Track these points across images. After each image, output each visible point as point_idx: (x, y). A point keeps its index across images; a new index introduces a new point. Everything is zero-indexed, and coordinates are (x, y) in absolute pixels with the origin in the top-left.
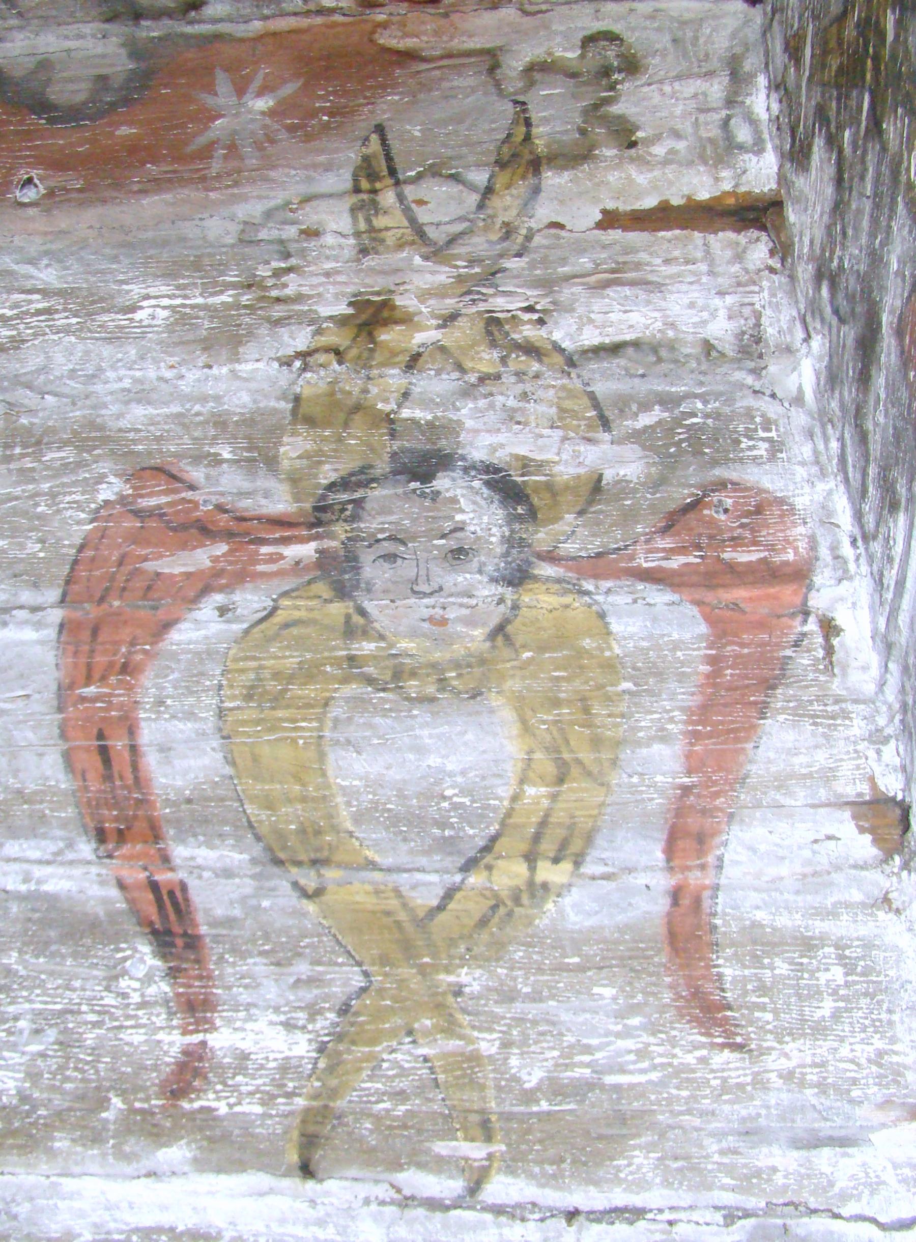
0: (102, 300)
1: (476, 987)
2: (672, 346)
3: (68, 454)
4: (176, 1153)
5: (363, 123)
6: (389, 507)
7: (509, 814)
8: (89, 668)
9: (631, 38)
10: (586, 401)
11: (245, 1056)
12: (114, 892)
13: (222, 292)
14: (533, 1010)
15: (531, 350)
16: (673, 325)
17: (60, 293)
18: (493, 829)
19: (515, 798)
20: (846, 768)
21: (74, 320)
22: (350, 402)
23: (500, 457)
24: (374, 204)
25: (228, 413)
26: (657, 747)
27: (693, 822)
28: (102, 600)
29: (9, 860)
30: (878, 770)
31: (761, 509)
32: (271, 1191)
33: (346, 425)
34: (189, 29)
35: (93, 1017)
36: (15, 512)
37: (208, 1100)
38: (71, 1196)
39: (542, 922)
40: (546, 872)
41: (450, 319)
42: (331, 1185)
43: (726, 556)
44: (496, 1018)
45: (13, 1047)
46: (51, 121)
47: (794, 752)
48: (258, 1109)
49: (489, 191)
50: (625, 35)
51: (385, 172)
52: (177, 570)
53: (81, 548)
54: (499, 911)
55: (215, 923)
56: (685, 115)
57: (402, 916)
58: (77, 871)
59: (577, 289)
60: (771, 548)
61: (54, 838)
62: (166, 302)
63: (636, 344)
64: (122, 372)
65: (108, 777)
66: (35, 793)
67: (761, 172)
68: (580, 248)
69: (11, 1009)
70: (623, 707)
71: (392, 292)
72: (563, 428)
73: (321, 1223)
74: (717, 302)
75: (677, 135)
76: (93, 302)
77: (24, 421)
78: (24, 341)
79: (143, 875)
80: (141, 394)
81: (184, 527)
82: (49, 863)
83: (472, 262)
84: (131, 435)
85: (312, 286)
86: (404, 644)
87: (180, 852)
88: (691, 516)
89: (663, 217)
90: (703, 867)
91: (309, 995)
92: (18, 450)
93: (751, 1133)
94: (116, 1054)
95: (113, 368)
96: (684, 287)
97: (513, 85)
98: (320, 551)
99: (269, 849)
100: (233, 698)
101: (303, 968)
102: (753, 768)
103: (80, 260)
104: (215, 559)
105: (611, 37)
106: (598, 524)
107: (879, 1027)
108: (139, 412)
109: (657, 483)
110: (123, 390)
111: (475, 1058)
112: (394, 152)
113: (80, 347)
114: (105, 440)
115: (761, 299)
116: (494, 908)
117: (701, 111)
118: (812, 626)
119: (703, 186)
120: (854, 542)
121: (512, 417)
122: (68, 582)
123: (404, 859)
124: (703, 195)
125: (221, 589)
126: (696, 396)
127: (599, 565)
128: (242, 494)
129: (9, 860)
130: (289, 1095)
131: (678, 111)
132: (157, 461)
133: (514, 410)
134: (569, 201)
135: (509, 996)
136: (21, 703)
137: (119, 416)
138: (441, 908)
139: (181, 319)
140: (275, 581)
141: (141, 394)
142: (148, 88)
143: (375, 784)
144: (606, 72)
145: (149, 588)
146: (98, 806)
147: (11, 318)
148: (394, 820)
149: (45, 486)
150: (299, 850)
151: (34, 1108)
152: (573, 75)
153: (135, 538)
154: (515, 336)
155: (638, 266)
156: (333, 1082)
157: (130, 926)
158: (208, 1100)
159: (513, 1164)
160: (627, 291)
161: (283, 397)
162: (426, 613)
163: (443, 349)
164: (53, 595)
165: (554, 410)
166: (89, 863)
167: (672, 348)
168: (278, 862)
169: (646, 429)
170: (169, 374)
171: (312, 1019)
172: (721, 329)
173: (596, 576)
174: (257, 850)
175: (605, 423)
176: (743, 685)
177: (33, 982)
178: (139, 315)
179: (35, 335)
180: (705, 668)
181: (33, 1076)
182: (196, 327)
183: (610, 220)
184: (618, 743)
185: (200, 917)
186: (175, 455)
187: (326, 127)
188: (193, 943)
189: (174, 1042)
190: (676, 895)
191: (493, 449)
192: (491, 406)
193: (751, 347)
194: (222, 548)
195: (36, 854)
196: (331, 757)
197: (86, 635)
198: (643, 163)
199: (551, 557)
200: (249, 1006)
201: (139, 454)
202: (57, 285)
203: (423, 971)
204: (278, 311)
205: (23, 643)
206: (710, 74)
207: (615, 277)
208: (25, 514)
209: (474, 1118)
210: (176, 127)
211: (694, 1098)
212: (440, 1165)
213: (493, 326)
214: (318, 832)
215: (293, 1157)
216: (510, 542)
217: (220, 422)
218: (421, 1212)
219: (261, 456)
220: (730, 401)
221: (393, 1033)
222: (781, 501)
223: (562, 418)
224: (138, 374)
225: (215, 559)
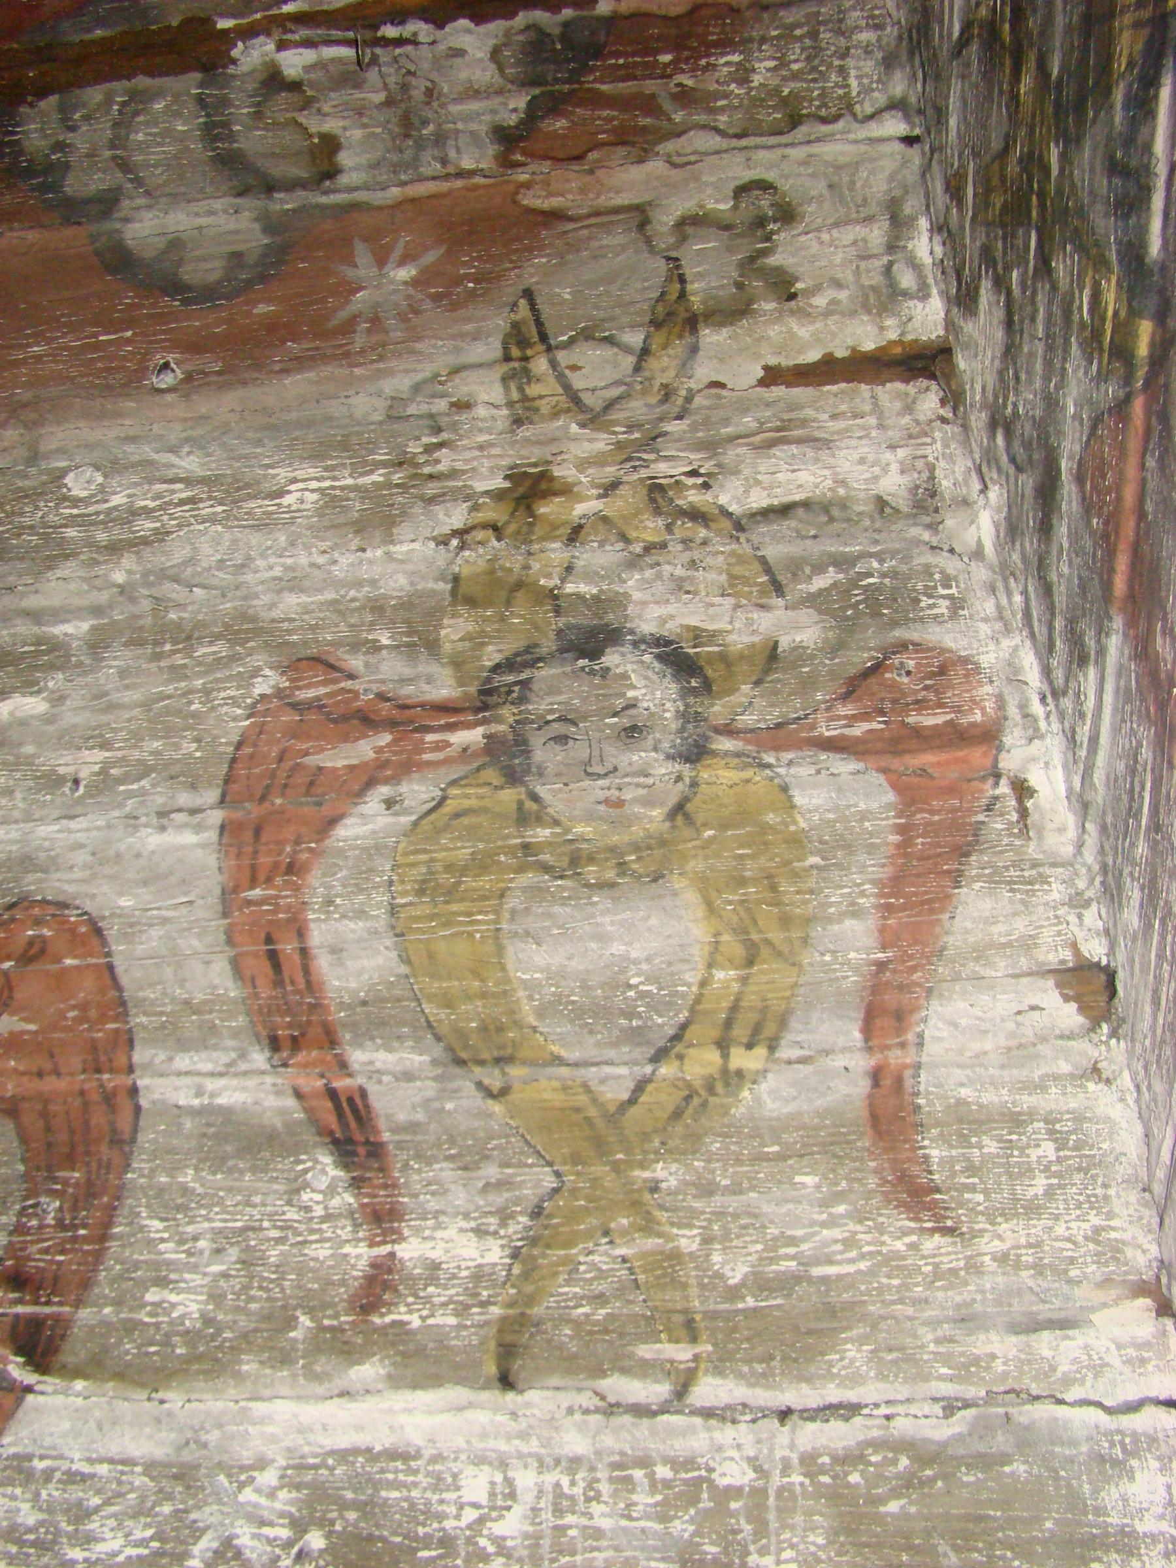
0: (248, 486)
1: (673, 1182)
2: (843, 505)
3: (220, 648)
4: (368, 1371)
5: (510, 289)
6: (556, 688)
7: (698, 1000)
8: (254, 869)
9: (784, 185)
10: (757, 566)
11: (435, 1266)
12: (291, 1102)
13: (372, 472)
14: (734, 1203)
15: (697, 515)
16: (843, 483)
17: (203, 481)
18: (682, 1017)
19: (703, 983)
20: (1047, 935)
21: (220, 509)
22: (512, 579)
23: (670, 629)
24: (526, 372)
25: (385, 597)
26: (848, 923)
27: (890, 999)
28: (263, 798)
29: (179, 1074)
30: (1080, 936)
31: (946, 669)
32: (470, 1405)
33: (508, 603)
34: (324, 200)
35: (275, 1234)
36: (168, 711)
37: (399, 1314)
38: (262, 1421)
39: (738, 1111)
40: (740, 1059)
41: (610, 488)
42: (532, 1395)
43: (910, 720)
44: (695, 1214)
45: (194, 1269)
46: (186, 302)
47: (992, 920)
48: (452, 1321)
49: (645, 352)
50: (779, 183)
51: (536, 339)
52: (339, 764)
53: (239, 745)
54: (693, 1102)
55: (397, 1129)
56: (845, 263)
57: (593, 1112)
58: (252, 1082)
60: (958, 709)
61: (225, 1049)
62: (314, 485)
63: (806, 504)
64: (272, 560)
65: (279, 983)
66: (204, 1002)
67: (928, 318)
68: (743, 407)
69: (190, 1229)
70: (811, 883)
71: (549, 463)
72: (735, 595)
73: (524, 1436)
74: (888, 456)
75: (838, 284)
76: (239, 489)
77: (173, 616)
78: (168, 533)
79: (320, 1083)
80: (293, 582)
81: (345, 718)
82: (221, 1075)
83: (631, 428)
84: (285, 625)
85: (466, 461)
86: (579, 829)
87: (357, 1057)
88: (872, 680)
89: (826, 371)
90: (903, 1045)
91: (499, 1199)
92: (168, 647)
93: (967, 1319)
94: (301, 1270)
95: (263, 556)
96: (853, 443)
97: (664, 239)
98: (488, 737)
99: (450, 1049)
100: (405, 893)
101: (491, 1171)
102: (950, 940)
103: (223, 445)
104: (379, 750)
105: (764, 186)
106: (776, 693)
107: (1097, 1203)
108: (292, 601)
109: (835, 648)
110: (275, 579)
111: (675, 1256)
112: (544, 316)
113: (227, 536)
114: (258, 632)
116: (688, 1098)
117: (862, 258)
118: (1004, 788)
119: (867, 336)
120: (1043, 699)
121: (680, 587)
122: (227, 782)
123: (592, 1053)
124: (869, 346)
125: (387, 781)
126: (871, 555)
127: (779, 736)
128: (403, 681)
129: (179, 1074)
130: (484, 1304)
131: (838, 259)
132: (313, 651)
133: (682, 579)
134: (728, 359)
135: (708, 1190)
136: (184, 910)
137: (272, 606)
138: (632, 1101)
139: (331, 501)
140: (443, 770)
141: (293, 582)
142: (284, 263)
143: (557, 976)
144: (760, 222)
145: (312, 783)
146: (270, 1013)
147: (154, 510)
148: (579, 1012)
149: (198, 683)
150: (481, 1048)
151: (219, 1331)
152: (727, 228)
153: (295, 732)
154: (680, 502)
155: (804, 423)
156: (529, 1288)
157: (310, 1137)
158: (399, 1314)
159: (721, 1364)
160: (794, 449)
161: (442, 577)
162: (601, 795)
163: (605, 520)
164: (212, 795)
165: (724, 577)
166: (263, 1073)
167: (844, 507)
168: (460, 1062)
170: (321, 560)
171: (503, 1223)
172: (894, 484)
173: (777, 748)
174: (438, 1050)
175: (778, 589)
176: (934, 857)
177: (211, 1200)
178: (287, 500)
179: (180, 526)
180: (894, 838)
181: (216, 1297)
182: (348, 509)
183: (772, 376)
184: (808, 921)
185: (382, 1124)
186: (332, 644)
187: (472, 294)
188: (376, 1150)
189: (361, 1255)
190: (876, 1075)
191: (663, 621)
192: (659, 576)
193: (927, 501)
194: (385, 738)
195: (208, 1067)
196: (510, 950)
197: (248, 835)
198: (804, 315)
199: (729, 731)
200: (437, 1214)
201: (294, 644)
202: (200, 472)
203: (616, 1167)
204: (431, 489)
205: (183, 847)
206: (869, 219)
207: (781, 434)
208: (179, 712)
209: (678, 1319)
210: (316, 302)
211: (905, 1286)
212: (644, 1369)
213: (656, 492)
214: (500, 1029)
215: (492, 1369)
216: (686, 717)
217: (377, 607)
218: (627, 1419)
219: (421, 641)
220: (906, 559)
221: (589, 1234)
222: (965, 661)
223: (733, 585)
224: (289, 561)
225: (379, 750)
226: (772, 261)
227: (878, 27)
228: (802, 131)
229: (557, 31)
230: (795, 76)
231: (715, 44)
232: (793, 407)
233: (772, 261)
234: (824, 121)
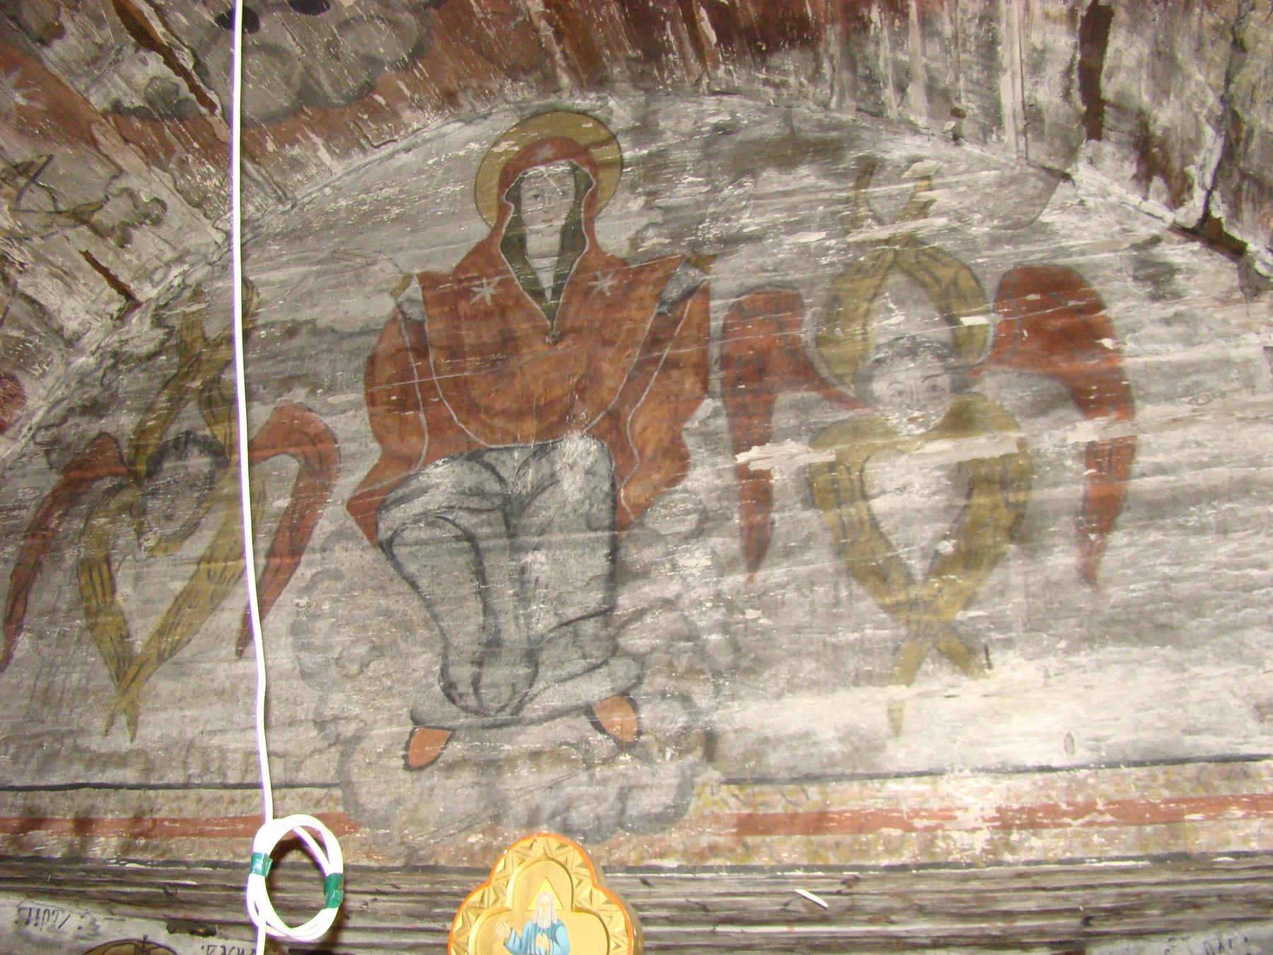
2: (50, 318)
5: (46, 149)
9: (169, 213)
16: (60, 311)
24: (15, 176)
49: (60, 213)
59: (46, 270)
63: (41, 307)
67: (146, 292)
68: (66, 254)
75: (139, 258)
83: (24, 227)
89: (105, 271)
105: (164, 206)
115: (96, 325)
117: (157, 257)
120: (30, 429)
124: (122, 279)
131: (151, 250)
134: (80, 238)
144: (147, 216)
152: (136, 207)
155: (75, 278)
160: (61, 284)
169: (12, 337)
172: (72, 326)
183: (87, 255)
187: (34, 135)
193: (72, 343)
198: (117, 254)
206: (175, 248)
207: (65, 277)
222: (24, 398)
226: (133, 231)
227: (258, 210)
228: (197, 210)
229: (182, 97)
230: (218, 195)
231: (213, 158)
232: (79, 268)
233: (133, 231)
234: (206, 215)
